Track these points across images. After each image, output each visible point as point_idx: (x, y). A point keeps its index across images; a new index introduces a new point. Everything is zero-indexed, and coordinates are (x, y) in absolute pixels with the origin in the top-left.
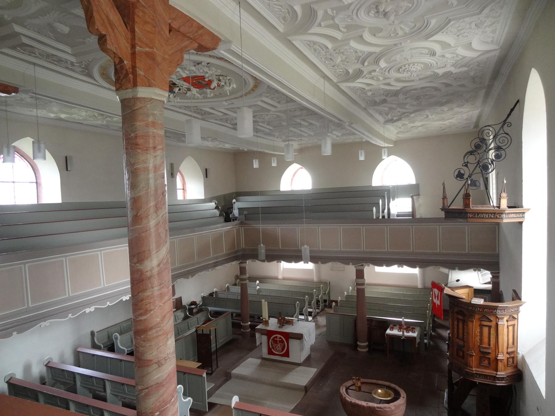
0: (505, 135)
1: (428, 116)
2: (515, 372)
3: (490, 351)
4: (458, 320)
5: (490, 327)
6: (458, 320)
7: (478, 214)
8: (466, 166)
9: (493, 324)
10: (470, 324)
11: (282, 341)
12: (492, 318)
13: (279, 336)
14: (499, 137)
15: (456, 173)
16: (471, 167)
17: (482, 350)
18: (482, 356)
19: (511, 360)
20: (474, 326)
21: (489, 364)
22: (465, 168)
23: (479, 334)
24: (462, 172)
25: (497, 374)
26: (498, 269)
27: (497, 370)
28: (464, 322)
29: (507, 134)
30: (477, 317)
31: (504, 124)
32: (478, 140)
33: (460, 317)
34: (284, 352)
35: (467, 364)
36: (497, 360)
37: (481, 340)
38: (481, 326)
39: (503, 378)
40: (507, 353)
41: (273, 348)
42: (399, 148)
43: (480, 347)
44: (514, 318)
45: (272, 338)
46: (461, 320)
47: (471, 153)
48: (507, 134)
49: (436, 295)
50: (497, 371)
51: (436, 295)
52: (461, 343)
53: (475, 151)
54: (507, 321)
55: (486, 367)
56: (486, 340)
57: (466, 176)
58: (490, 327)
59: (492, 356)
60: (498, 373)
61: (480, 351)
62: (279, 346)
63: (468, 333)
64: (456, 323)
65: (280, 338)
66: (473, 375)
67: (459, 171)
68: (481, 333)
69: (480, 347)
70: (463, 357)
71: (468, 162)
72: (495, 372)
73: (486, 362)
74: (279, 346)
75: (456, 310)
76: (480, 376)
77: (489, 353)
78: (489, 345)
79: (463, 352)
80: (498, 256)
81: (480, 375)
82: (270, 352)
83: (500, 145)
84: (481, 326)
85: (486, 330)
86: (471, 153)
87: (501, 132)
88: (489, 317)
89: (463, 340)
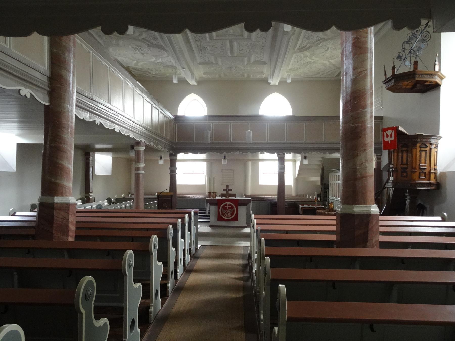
0: (427, 33)
1: (328, 48)
6: (402, 152)
7: (422, 74)
8: (404, 51)
9: (428, 149)
10: (414, 151)
11: (231, 207)
12: (428, 145)
13: (228, 203)
14: (424, 34)
15: (397, 55)
16: (407, 52)
21: (425, 176)
22: (403, 52)
24: (401, 55)
27: (429, 180)
29: (428, 32)
30: (418, 145)
31: (426, 26)
32: (411, 34)
34: (233, 216)
36: (430, 172)
37: (420, 161)
41: (223, 214)
42: (282, 88)
45: (222, 206)
46: (405, 151)
47: (407, 42)
48: (428, 32)
49: (389, 135)
51: (389, 135)
52: (406, 166)
53: (409, 41)
56: (423, 160)
57: (403, 58)
59: (427, 171)
61: (420, 168)
62: (229, 212)
65: (230, 205)
67: (399, 55)
68: (420, 156)
69: (419, 165)
71: (405, 49)
73: (423, 175)
74: (229, 212)
78: (426, 163)
82: (220, 218)
83: (425, 39)
85: (423, 154)
86: (407, 42)
87: (425, 30)
89: (407, 164)
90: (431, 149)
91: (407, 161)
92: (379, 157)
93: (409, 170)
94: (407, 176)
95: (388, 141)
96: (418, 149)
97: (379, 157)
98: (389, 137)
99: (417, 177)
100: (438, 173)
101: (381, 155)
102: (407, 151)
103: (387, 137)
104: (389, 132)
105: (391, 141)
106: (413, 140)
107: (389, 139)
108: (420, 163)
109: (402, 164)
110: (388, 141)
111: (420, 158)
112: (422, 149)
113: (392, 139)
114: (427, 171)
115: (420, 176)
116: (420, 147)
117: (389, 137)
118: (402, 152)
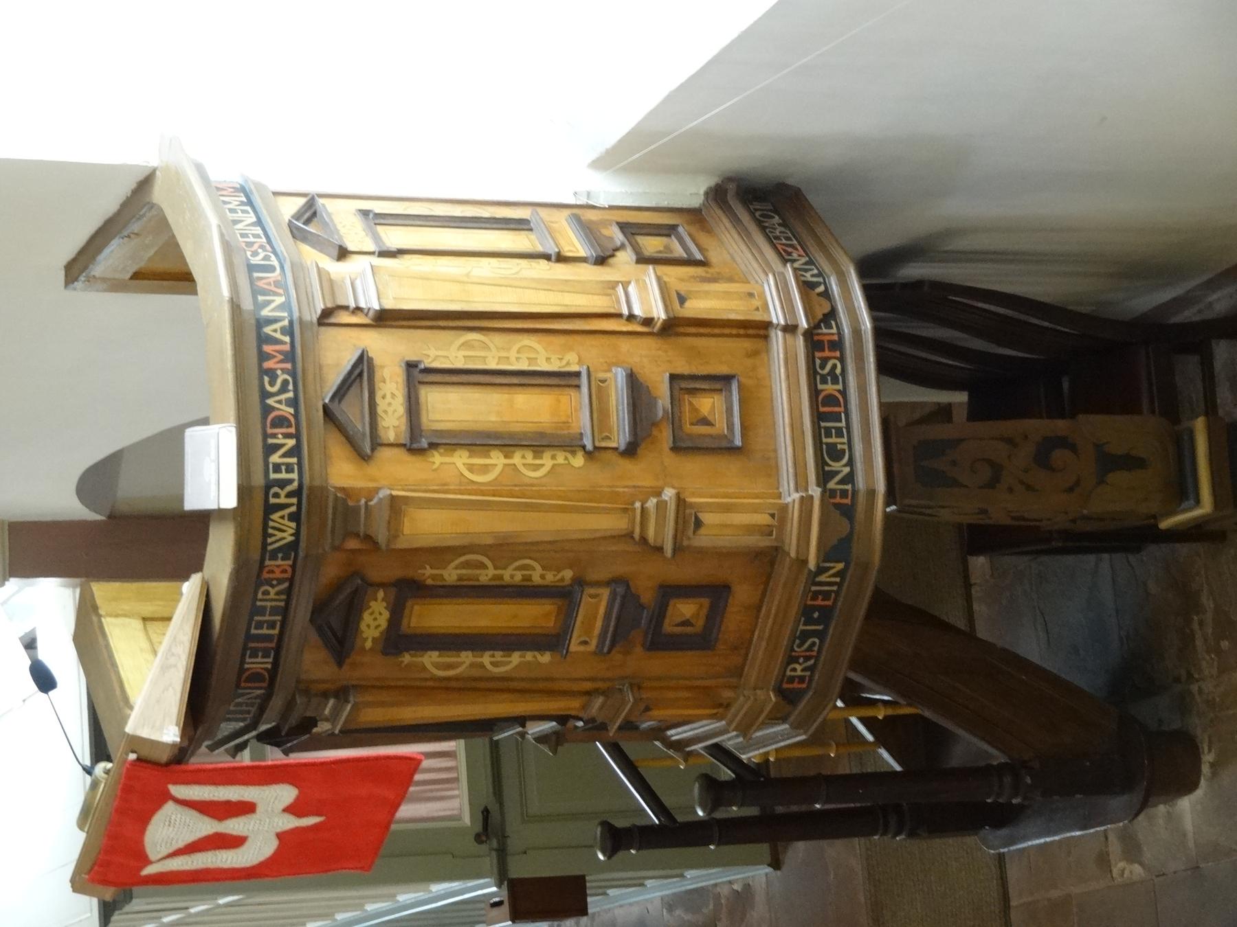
2: (736, 221)
3: (618, 378)
4: (398, 640)
5: (418, 375)
10: (426, 526)
12: (337, 352)
17: (620, 436)
18: (665, 436)
19: (652, 245)
20: (437, 497)
23: (497, 459)
25: (790, 329)
27: (758, 330)
28: (409, 590)
30: (343, 472)
33: (374, 620)
35: (765, 559)
37: (539, 443)
38: (419, 442)
39: (806, 287)
40: (601, 261)
43: (591, 455)
44: (310, 212)
49: (206, 827)
50: (767, 325)
51: (206, 827)
52: (595, 608)
54: (343, 253)
55: (753, 404)
56: (531, 409)
58: (418, 375)
59: (657, 364)
60: (777, 316)
61: (631, 451)
63: (503, 549)
64: (431, 660)
66: (841, 505)
68: (480, 441)
70: (716, 593)
72: (778, 338)
73: (707, 404)
75: (313, 662)
76: (836, 455)
77: (634, 383)
78: (564, 380)
79: (670, 592)
81: (827, 453)
84: (419, 442)
85: (447, 408)
88: (334, 379)
90: (385, 319)
91: (526, 592)
93: (647, 578)
94: (717, 593)
95: (280, 836)
96: (394, 474)
98: (233, 826)
99: (729, 468)
100: (612, 191)
102: (409, 590)
103: (235, 842)
106: (284, 531)
108: (571, 444)
109: (553, 641)
111: (505, 442)
112: (392, 419)
115: (724, 449)
116: (365, 447)
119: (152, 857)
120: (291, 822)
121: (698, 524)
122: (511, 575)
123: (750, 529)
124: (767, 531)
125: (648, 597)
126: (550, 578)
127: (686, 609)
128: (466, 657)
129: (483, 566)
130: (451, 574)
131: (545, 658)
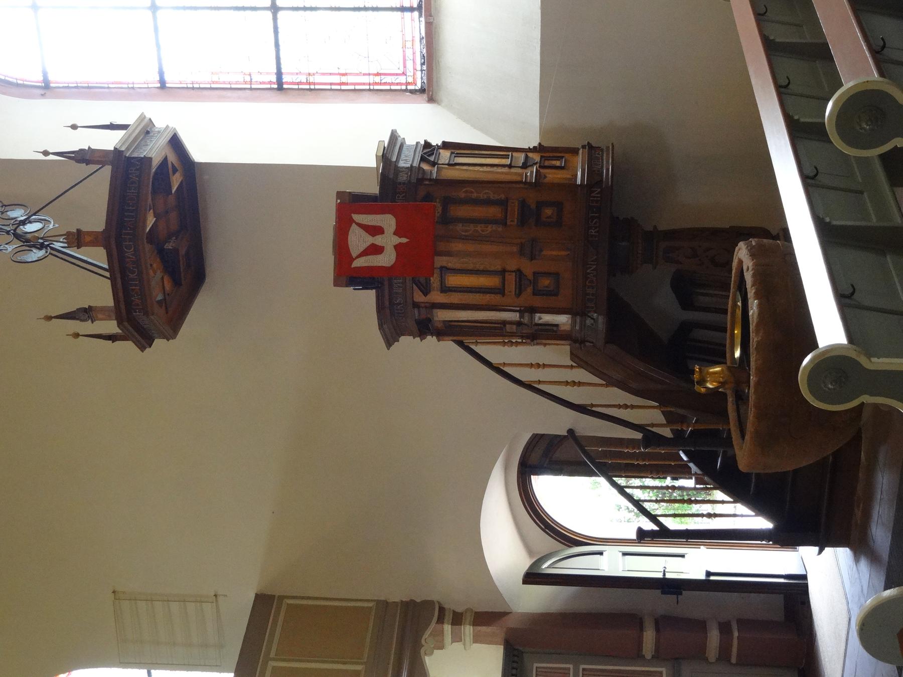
6: (446, 220)
26: (428, 605)
46: (445, 210)
49: (369, 240)
51: (369, 240)
52: (514, 208)
64: (459, 227)
70: (559, 205)
72: (581, 151)
79: (540, 205)
80: (384, 606)
90: (446, 145)
91: (488, 202)
92: (449, 617)
94: (559, 205)
95: (397, 247)
97: (449, 617)
98: (379, 240)
101: (442, 610)
102: (447, 202)
104: (358, 240)
105: (396, 233)
107: (389, 240)
110: (397, 247)
113: (388, 222)
114: (536, 157)
117: (379, 240)
118: (446, 220)
119: (354, 255)
120: (397, 240)
121: (545, 177)
122: (483, 196)
123: (566, 179)
124: (570, 179)
125: (533, 206)
126: (497, 197)
127: (548, 211)
128: (472, 227)
129: (472, 192)
130: (462, 195)
131: (500, 229)
